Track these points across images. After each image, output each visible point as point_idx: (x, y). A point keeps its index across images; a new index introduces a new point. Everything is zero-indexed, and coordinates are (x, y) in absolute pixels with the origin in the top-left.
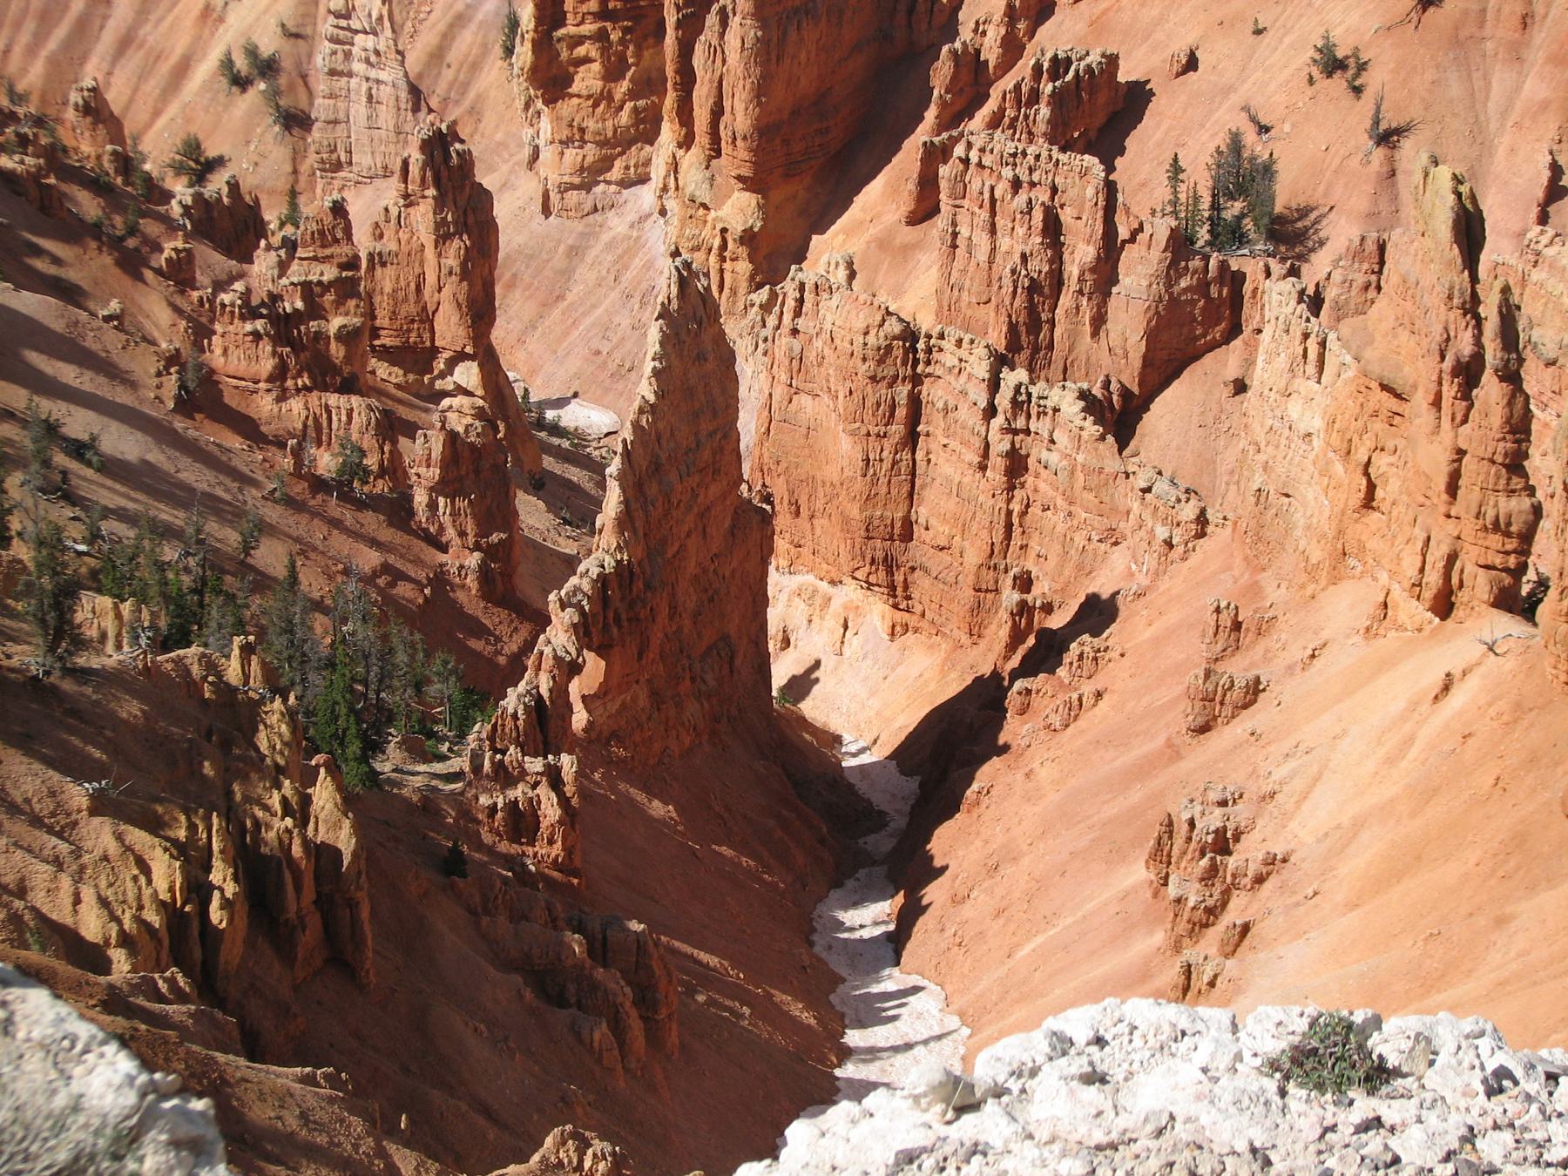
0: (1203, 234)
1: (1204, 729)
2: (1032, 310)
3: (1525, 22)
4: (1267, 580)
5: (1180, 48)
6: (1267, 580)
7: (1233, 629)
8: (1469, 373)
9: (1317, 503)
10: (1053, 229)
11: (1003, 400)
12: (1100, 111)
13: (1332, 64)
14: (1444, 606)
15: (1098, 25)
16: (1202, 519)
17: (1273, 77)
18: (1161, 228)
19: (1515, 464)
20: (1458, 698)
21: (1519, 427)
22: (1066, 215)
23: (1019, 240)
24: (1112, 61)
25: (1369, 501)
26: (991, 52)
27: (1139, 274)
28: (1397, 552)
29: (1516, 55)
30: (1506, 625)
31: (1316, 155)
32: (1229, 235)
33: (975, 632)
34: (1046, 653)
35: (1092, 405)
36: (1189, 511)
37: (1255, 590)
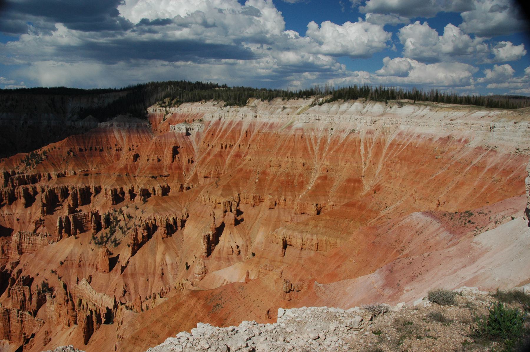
0: (42, 292)
1: (45, 345)
2: (23, 304)
3: (72, 264)
4: (51, 327)
5: (37, 273)
6: (51, 327)
7: (47, 333)
8: (67, 301)
9: (55, 318)
10: (24, 295)
11: (19, 314)
12: (28, 281)
13: (53, 272)
14: (69, 325)
15: (27, 272)
16: (44, 322)
17: (47, 274)
18: (37, 292)
19: (74, 309)
20: (72, 335)
21: (73, 305)
22: (25, 293)
23: (20, 297)
24: (29, 276)
25: (60, 316)
26: (15, 277)
27: (35, 298)
28: (63, 321)
29: (72, 268)
30: (75, 326)
31: (52, 281)
32: (44, 291)
33: (20, 341)
34: (27, 341)
35: (30, 313)
36: (42, 321)
37: (50, 328)
